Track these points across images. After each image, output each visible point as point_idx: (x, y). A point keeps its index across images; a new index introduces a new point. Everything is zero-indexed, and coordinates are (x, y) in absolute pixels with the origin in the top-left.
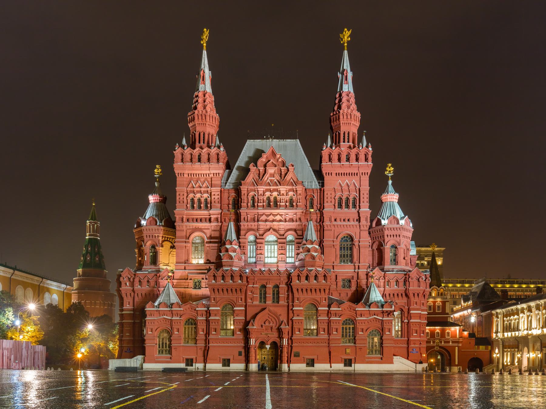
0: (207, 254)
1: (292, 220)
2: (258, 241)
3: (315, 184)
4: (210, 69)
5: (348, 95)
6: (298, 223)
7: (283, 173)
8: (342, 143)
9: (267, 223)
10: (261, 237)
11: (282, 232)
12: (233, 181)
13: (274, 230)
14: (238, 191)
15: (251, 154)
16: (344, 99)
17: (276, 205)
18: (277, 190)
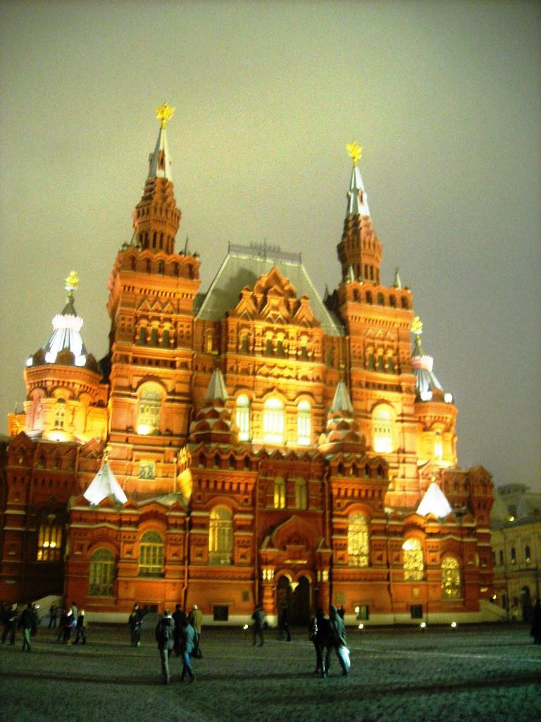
1: (305, 378)
3: (332, 327)
6: (316, 384)
7: (292, 307)
9: (271, 379)
10: (258, 400)
11: (292, 395)
13: (280, 391)
16: (362, 224)
17: (282, 353)
18: (283, 330)
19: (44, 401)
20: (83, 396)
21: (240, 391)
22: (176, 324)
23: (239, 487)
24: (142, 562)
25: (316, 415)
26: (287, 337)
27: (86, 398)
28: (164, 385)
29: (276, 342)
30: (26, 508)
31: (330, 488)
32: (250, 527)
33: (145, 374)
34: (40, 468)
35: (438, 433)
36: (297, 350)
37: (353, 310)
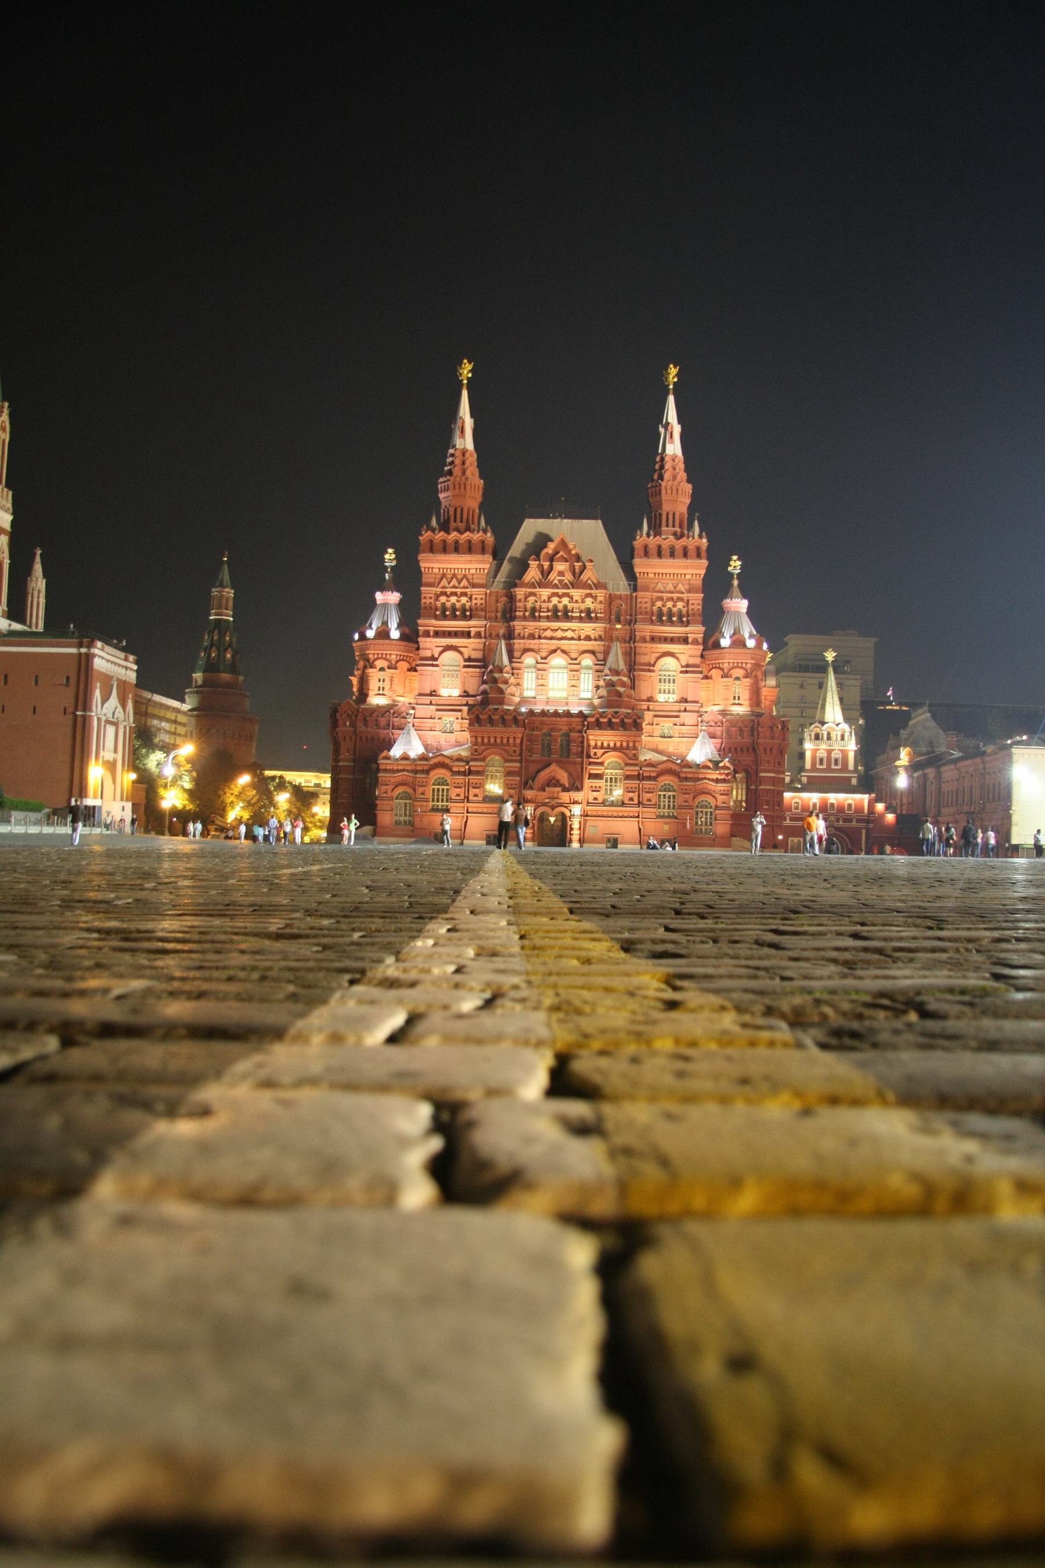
0: (464, 683)
1: (588, 638)
2: (539, 666)
3: (620, 585)
4: (473, 415)
5: (673, 460)
8: (664, 528)
11: (574, 655)
13: (563, 651)
16: (668, 466)
22: (471, 598)
27: (404, 665)
28: (461, 653)
29: (560, 607)
30: (354, 760)
31: (588, 740)
32: (517, 773)
34: (363, 727)
35: (737, 679)
36: (581, 612)
37: (640, 565)
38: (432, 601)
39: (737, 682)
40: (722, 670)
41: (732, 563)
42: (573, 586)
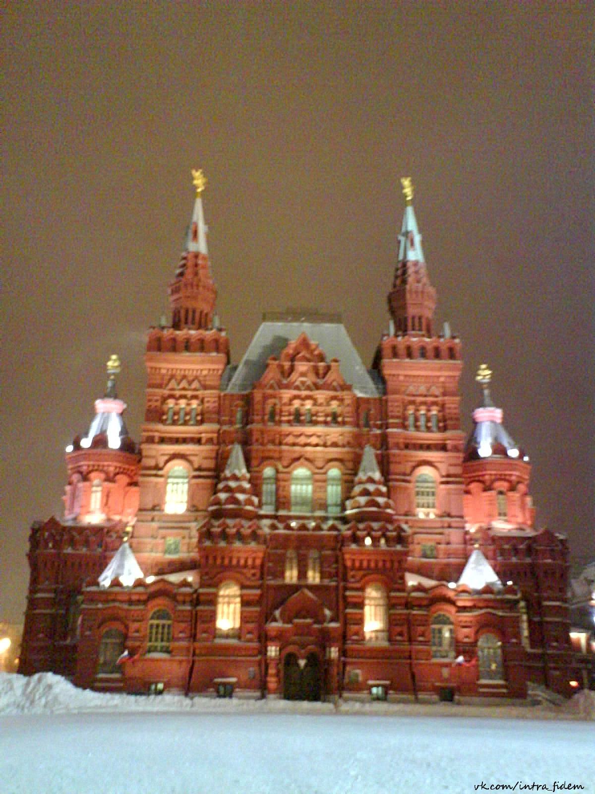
1: (335, 445)
4: (207, 222)
7: (321, 372)
9: (297, 448)
11: (320, 464)
12: (238, 382)
13: (307, 459)
14: (248, 400)
15: (268, 341)
19: (81, 485)
20: (118, 477)
21: (265, 463)
22: (202, 401)
23: (246, 561)
24: (150, 641)
25: (346, 481)
26: (315, 404)
27: (123, 479)
31: (343, 559)
33: (172, 452)
34: (69, 550)
36: (327, 415)
37: (390, 367)
38: (158, 404)
39: (501, 497)
40: (483, 482)
41: (480, 372)
42: (317, 387)
